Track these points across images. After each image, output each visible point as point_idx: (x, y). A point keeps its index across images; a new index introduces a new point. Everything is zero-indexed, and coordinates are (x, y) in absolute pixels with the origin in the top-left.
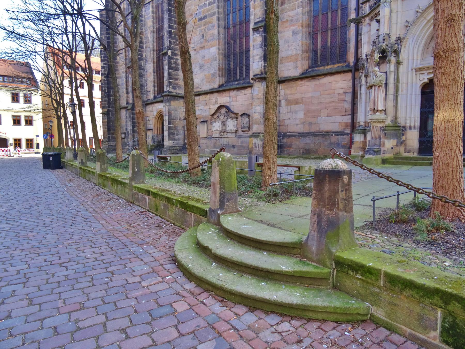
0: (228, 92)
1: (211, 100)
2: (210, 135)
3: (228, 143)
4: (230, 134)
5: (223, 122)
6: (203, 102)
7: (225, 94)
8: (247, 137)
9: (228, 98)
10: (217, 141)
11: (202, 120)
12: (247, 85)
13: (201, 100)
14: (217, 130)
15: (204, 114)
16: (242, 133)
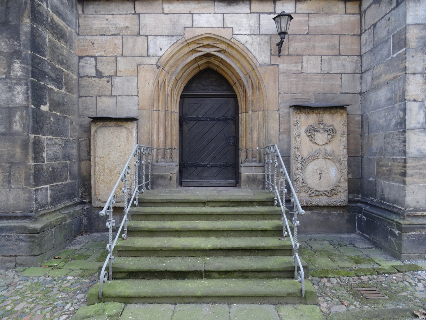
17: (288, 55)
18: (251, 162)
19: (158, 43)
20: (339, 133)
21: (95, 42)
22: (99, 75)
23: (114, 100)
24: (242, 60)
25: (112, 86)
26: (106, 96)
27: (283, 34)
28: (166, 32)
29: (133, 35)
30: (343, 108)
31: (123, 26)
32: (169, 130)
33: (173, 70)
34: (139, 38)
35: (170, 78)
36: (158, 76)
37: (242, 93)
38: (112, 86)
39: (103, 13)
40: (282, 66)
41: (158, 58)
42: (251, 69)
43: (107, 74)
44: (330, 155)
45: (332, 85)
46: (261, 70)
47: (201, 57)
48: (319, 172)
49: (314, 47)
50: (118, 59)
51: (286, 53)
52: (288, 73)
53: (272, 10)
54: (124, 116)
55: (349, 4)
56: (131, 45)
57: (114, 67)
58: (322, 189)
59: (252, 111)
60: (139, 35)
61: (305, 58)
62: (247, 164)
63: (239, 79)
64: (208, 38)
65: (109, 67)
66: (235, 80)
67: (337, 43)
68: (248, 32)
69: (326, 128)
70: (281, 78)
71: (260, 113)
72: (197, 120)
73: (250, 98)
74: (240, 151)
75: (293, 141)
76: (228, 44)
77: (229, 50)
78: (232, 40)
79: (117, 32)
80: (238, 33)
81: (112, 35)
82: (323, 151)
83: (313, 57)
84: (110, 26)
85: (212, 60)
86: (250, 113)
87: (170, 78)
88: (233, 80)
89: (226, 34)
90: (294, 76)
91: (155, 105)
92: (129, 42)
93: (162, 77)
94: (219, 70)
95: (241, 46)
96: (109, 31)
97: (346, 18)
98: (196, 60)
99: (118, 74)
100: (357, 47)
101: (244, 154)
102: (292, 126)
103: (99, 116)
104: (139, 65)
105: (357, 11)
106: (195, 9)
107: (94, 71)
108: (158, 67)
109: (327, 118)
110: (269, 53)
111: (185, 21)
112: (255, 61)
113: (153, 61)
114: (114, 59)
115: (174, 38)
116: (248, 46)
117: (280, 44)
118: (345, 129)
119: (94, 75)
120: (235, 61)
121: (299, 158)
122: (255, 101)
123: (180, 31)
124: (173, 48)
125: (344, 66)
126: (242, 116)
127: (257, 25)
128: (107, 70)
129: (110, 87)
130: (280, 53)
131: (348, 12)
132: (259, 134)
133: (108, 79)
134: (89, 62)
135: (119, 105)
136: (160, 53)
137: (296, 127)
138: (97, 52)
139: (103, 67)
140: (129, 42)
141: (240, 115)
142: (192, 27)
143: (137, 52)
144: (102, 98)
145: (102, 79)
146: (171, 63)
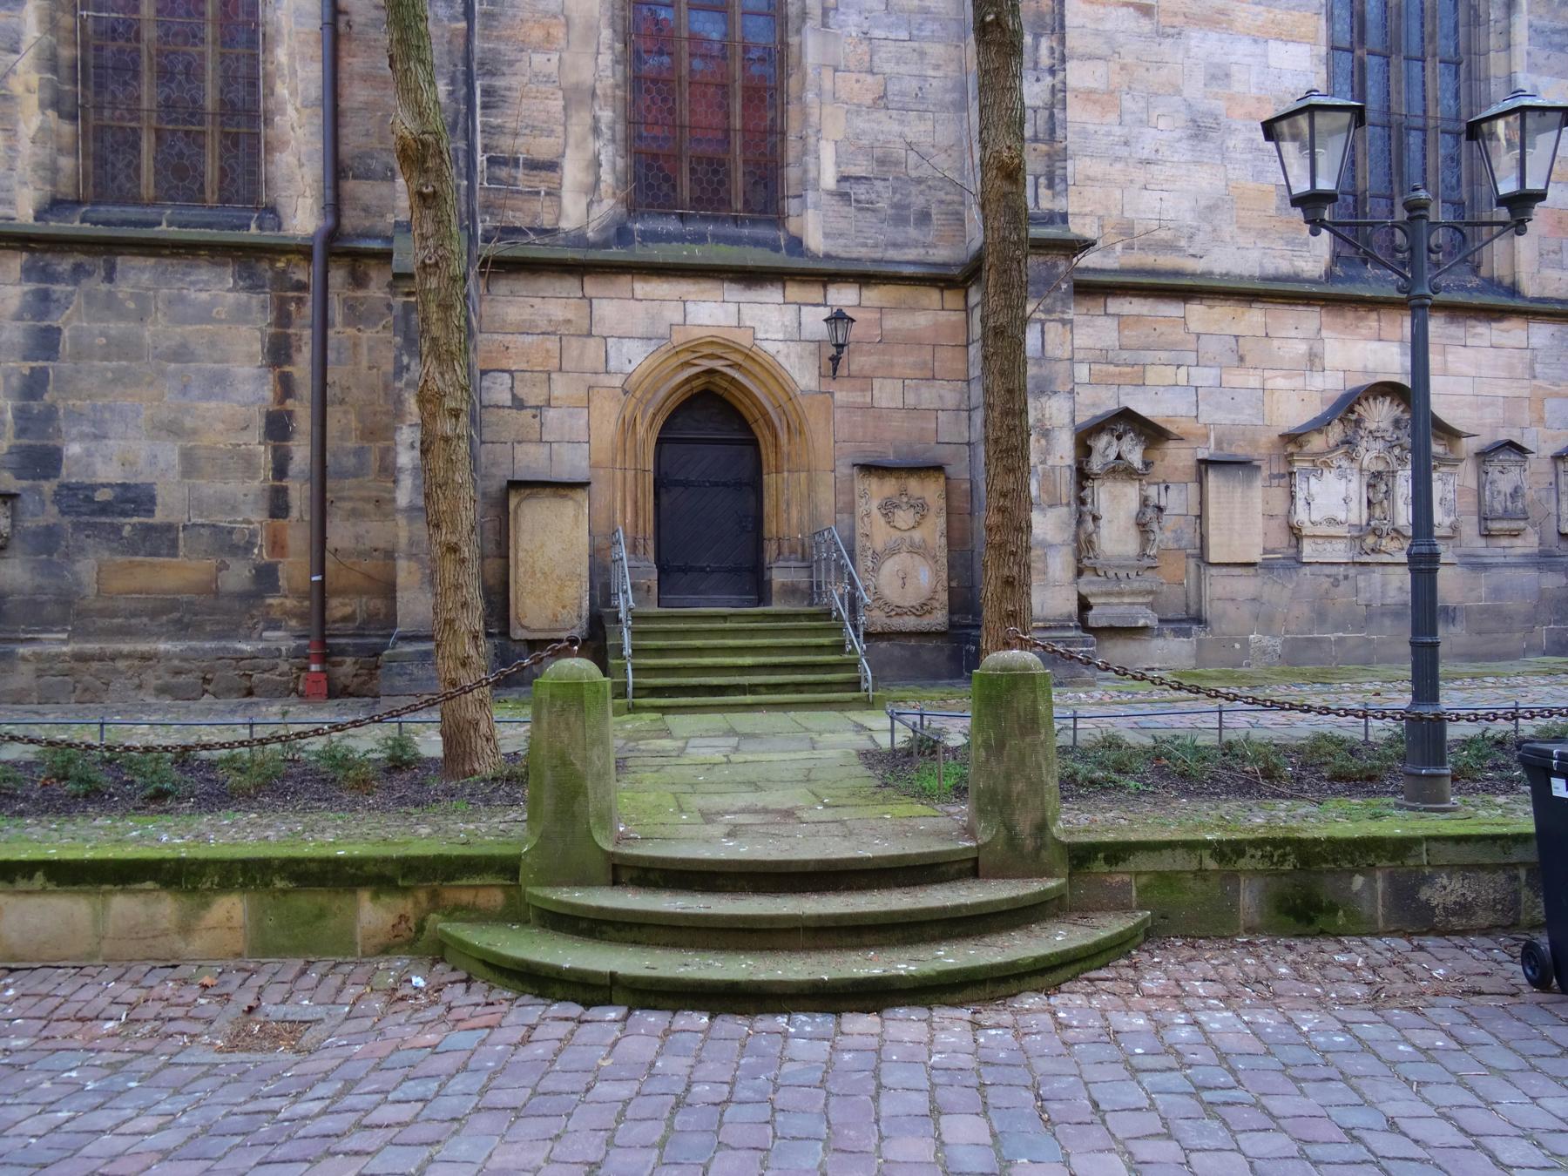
1: (1276, 343)
5: (1377, 475)
6: (1211, 347)
7: (1375, 324)
10: (1336, 583)
11: (1203, 454)
13: (1194, 326)
14: (1332, 521)
15: (1223, 418)
16: (1482, 542)
17: (849, 376)
18: (787, 560)
19: (624, 350)
20: (933, 510)
21: (511, 346)
22: (518, 404)
23: (545, 449)
24: (772, 383)
25: (542, 424)
26: (530, 441)
27: (840, 347)
28: (640, 331)
29: (579, 336)
30: (938, 469)
31: (561, 318)
32: (640, 503)
33: (649, 396)
34: (592, 342)
35: (644, 412)
36: (624, 407)
37: (770, 438)
38: (542, 424)
39: (525, 293)
40: (838, 396)
41: (624, 377)
42: (785, 398)
43: (532, 402)
44: (920, 547)
45: (922, 429)
46: (804, 402)
47: (697, 376)
48: (901, 574)
49: (892, 365)
50: (553, 376)
51: (845, 373)
52: (851, 408)
53: (820, 300)
54: (565, 478)
55: (947, 294)
56: (575, 353)
57: (545, 390)
58: (906, 604)
59: (789, 471)
60: (590, 335)
61: (877, 383)
62: (781, 564)
63: (765, 414)
64: (712, 343)
65: (536, 390)
66: (758, 416)
67: (929, 358)
68: (781, 336)
69: (912, 502)
70: (838, 416)
71: (803, 475)
72: (686, 484)
73: (785, 449)
74: (766, 542)
75: (859, 524)
76: (747, 355)
77: (747, 364)
78: (754, 349)
79: (550, 329)
80: (764, 336)
81: (543, 333)
82: (908, 540)
83: (889, 381)
84: (536, 317)
85: (717, 379)
86: (786, 474)
87: (644, 412)
88: (752, 414)
89: (744, 340)
90: (859, 412)
91: (619, 458)
92: (573, 348)
93: (630, 408)
94: (726, 395)
95: (769, 359)
96: (537, 326)
97: (943, 316)
98: (688, 381)
99: (553, 403)
100: (961, 366)
101: (774, 547)
102: (857, 497)
103: (516, 478)
104: (590, 387)
105: (961, 305)
106: (689, 293)
107: (509, 397)
108: (625, 393)
109: (914, 485)
110: (817, 373)
111: (672, 314)
112: (793, 385)
113: (617, 381)
114: (545, 376)
115: (653, 342)
116: (781, 359)
117: (835, 360)
118: (942, 503)
119: (509, 403)
120: (758, 383)
121: (870, 553)
122: (793, 454)
123: (663, 330)
124: (650, 360)
125: (941, 397)
126: (769, 480)
127: (796, 325)
128: (533, 396)
129: (537, 426)
130: (835, 370)
131: (946, 306)
132: (801, 512)
133: (534, 411)
134: (499, 381)
135: (554, 458)
136: (630, 369)
137: (863, 500)
138: (514, 363)
139: (526, 390)
140: (573, 348)
141: (765, 477)
142: (685, 324)
143: (588, 364)
144: (524, 445)
145: (524, 412)
146: (645, 385)
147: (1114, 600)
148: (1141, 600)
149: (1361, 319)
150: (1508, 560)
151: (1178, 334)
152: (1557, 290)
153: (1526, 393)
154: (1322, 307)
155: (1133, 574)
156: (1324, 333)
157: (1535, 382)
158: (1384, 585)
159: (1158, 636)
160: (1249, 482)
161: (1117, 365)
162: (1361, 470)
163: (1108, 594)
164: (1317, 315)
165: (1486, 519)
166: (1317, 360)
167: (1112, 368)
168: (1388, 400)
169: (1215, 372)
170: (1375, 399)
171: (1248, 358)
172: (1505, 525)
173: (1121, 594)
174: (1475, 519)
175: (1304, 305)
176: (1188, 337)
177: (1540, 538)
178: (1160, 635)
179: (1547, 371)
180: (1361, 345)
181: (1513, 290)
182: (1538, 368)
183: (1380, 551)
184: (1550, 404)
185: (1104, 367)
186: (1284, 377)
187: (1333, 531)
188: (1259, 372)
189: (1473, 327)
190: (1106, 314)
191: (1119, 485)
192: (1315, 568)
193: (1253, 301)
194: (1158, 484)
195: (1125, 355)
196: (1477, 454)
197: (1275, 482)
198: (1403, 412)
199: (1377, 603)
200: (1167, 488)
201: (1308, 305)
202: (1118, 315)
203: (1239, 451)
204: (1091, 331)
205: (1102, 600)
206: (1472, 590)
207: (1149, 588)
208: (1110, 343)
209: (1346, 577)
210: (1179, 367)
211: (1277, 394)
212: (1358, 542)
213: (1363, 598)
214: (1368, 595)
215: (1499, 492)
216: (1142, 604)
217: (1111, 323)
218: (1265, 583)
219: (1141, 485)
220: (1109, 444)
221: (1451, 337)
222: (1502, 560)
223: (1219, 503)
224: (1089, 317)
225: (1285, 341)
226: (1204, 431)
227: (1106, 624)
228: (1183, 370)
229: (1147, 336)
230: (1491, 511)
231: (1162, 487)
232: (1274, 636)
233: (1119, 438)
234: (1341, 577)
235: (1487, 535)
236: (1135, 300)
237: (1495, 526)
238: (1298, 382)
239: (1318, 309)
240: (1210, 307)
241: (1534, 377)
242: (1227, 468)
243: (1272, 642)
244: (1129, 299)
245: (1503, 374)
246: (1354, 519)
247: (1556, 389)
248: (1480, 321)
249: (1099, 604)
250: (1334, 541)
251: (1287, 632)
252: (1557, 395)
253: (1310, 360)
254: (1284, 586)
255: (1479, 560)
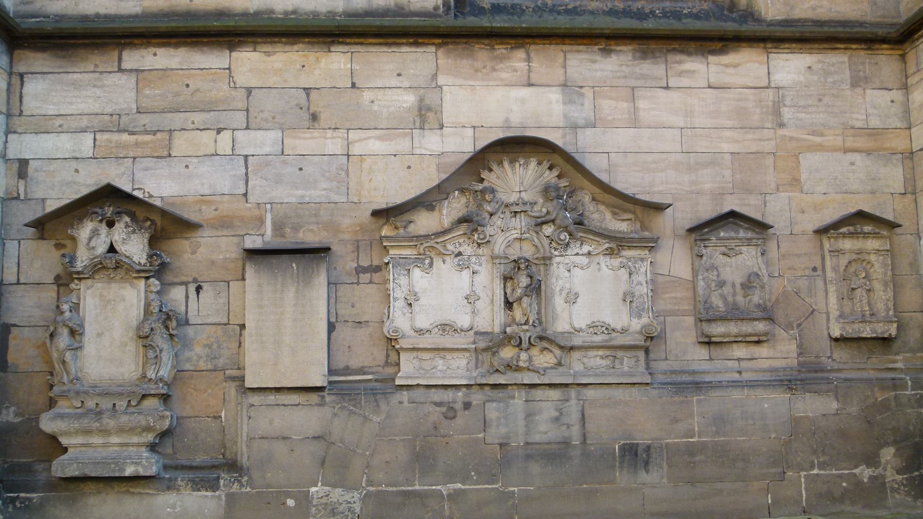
0: (555, 51)
1: (367, 96)
2: (347, 371)
3: (575, 433)
4: (596, 360)
6: (266, 103)
7: (522, 65)
8: (752, 385)
9: (554, 96)
10: (450, 413)
12: (730, 27)
13: (243, 78)
14: (446, 328)
15: (287, 195)
16: (703, 352)
147: (96, 440)
148: (135, 440)
149: (501, 59)
150: (746, 376)
151: (221, 90)
152: (814, 9)
153: (769, 146)
154: (438, 46)
155: (122, 404)
156: (441, 80)
157: (781, 132)
158: (529, 416)
159: (169, 488)
160: (306, 280)
161: (132, 133)
162: (493, 258)
163: (87, 432)
164: (431, 57)
165: (701, 321)
166: (431, 115)
167: (125, 137)
168: (533, 163)
169: (275, 135)
170: (512, 162)
171: (322, 116)
172: (733, 328)
173: (105, 432)
174: (690, 320)
175: (411, 44)
176: (234, 93)
177: (800, 346)
178: (170, 486)
179: (803, 115)
180: (501, 92)
181: (749, 15)
182: (787, 114)
183: (518, 369)
184: (809, 161)
185: (115, 137)
186: (379, 138)
187: (448, 341)
188: (341, 133)
189: (679, 62)
190: (120, 70)
191: (114, 286)
192: (418, 394)
193: (333, 43)
194: (186, 284)
195: (144, 119)
196: (691, 230)
197: (365, 277)
198: (559, 177)
199: (518, 441)
200: (198, 289)
201: (416, 44)
202: (137, 70)
203: (310, 237)
204: (98, 92)
205: (79, 440)
206: (675, 420)
207: (144, 423)
208: (125, 106)
209: (467, 406)
210: (219, 131)
211: (369, 160)
212: (486, 357)
213: (495, 434)
214: (503, 430)
215: (721, 284)
216: (139, 445)
217: (127, 82)
218: (335, 415)
219: (147, 286)
220: (95, 233)
221: (644, 77)
222: (736, 376)
223: (261, 307)
224: (97, 75)
225: (380, 94)
226: (256, 212)
227: (77, 473)
228: (226, 136)
229: (177, 94)
230: (707, 310)
231: (192, 288)
232: (348, 488)
233: (111, 224)
234: (459, 406)
235: (708, 342)
236: (161, 51)
237: (718, 330)
238: (403, 145)
239: (433, 49)
240: (268, 54)
241: (782, 125)
242: (274, 260)
243: (347, 497)
244: (152, 50)
245: (729, 123)
246: (483, 324)
247: (818, 139)
248: (689, 54)
249: (75, 446)
250: (449, 356)
251: (370, 483)
252: (820, 148)
253: (421, 115)
254: (366, 418)
255: (698, 378)
